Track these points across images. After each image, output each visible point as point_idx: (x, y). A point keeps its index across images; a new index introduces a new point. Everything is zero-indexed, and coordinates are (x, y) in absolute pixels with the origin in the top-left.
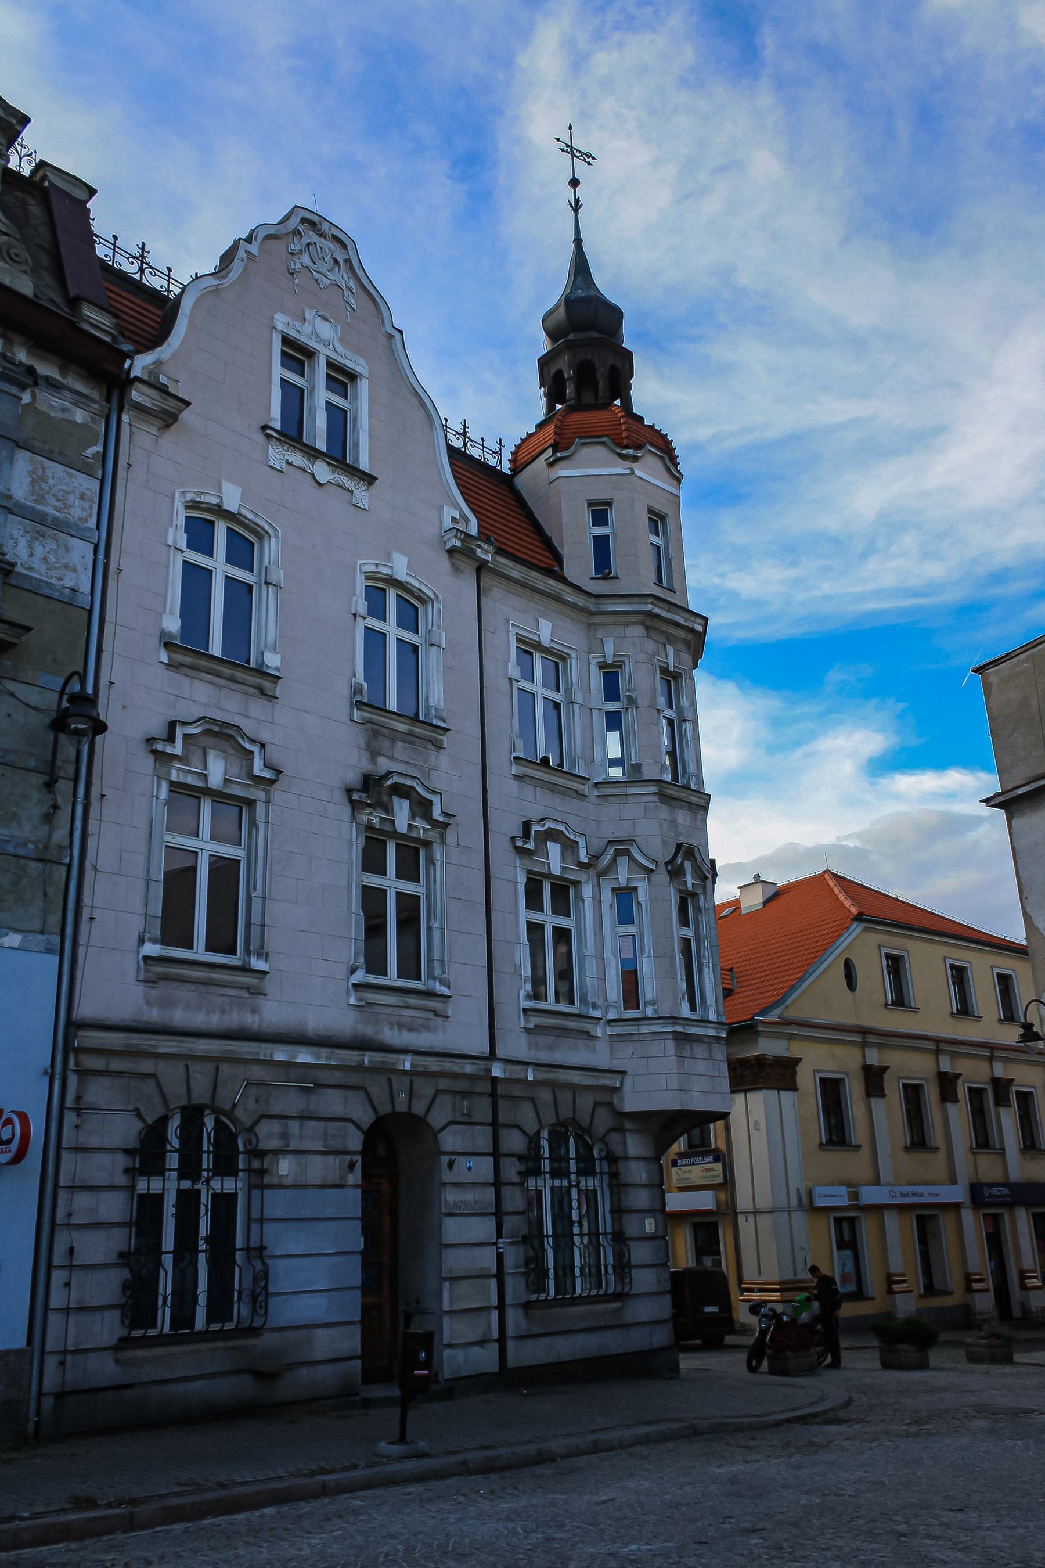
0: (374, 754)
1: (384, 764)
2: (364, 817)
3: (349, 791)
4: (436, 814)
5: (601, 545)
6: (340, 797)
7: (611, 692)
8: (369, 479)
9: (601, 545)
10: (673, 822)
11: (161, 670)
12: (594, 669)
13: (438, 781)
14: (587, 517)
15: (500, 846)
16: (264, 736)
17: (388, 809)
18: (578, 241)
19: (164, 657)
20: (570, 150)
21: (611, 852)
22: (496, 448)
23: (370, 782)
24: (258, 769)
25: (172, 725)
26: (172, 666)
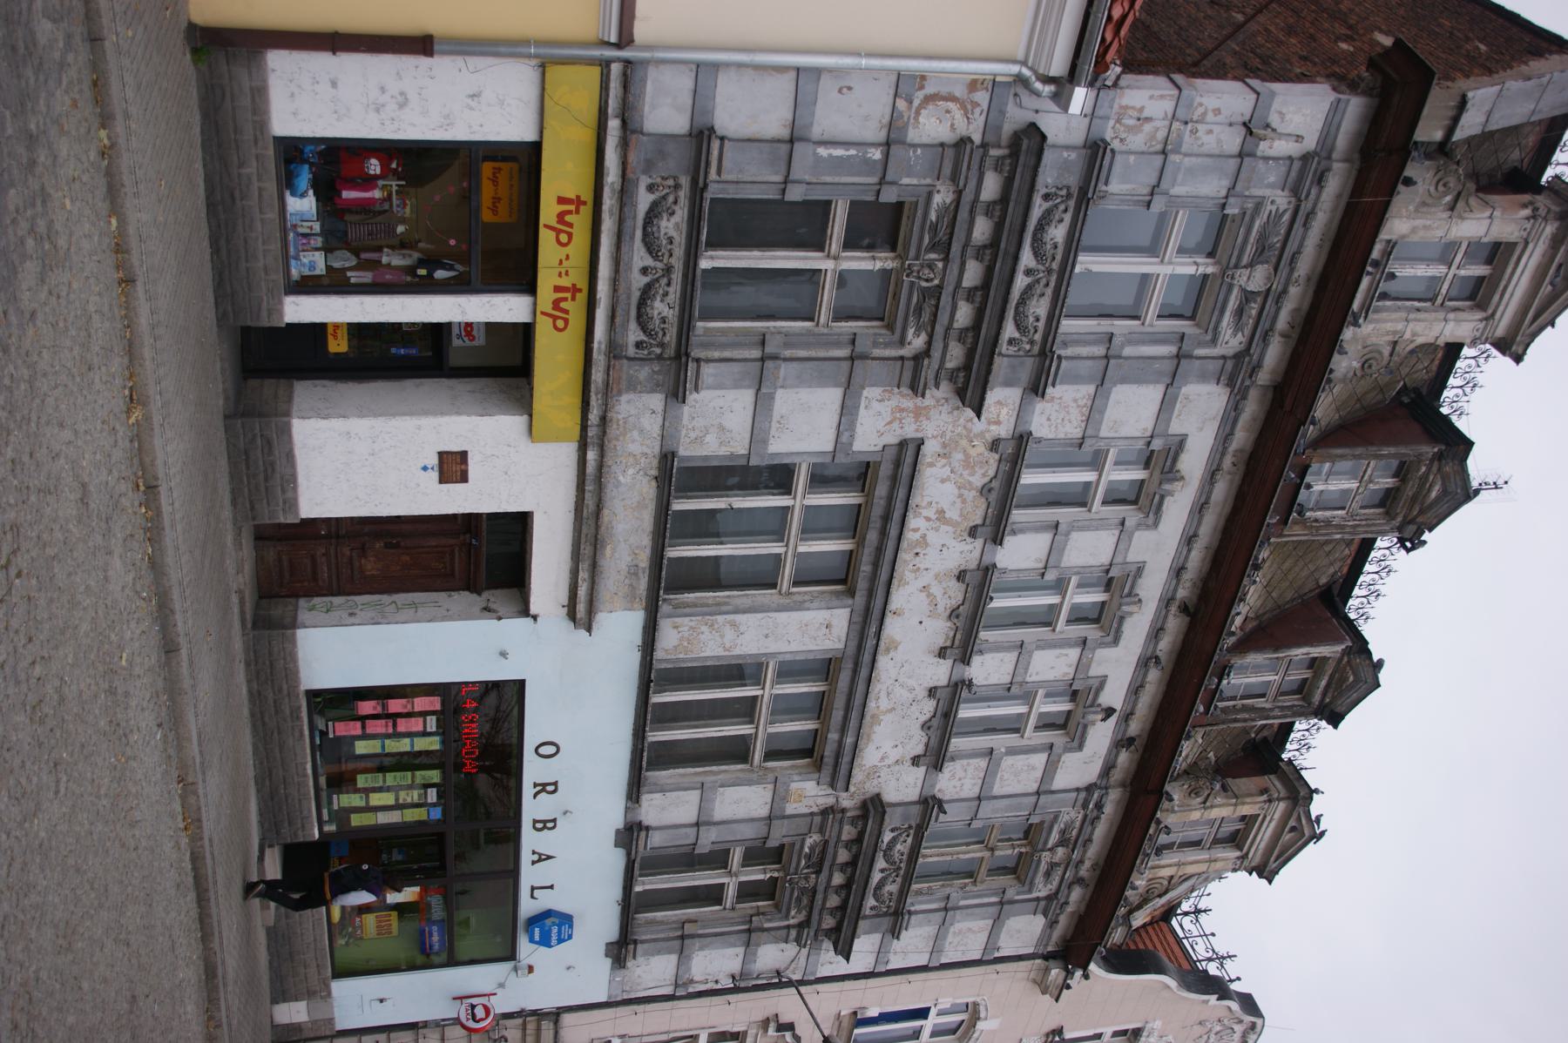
11: (834, 1011)
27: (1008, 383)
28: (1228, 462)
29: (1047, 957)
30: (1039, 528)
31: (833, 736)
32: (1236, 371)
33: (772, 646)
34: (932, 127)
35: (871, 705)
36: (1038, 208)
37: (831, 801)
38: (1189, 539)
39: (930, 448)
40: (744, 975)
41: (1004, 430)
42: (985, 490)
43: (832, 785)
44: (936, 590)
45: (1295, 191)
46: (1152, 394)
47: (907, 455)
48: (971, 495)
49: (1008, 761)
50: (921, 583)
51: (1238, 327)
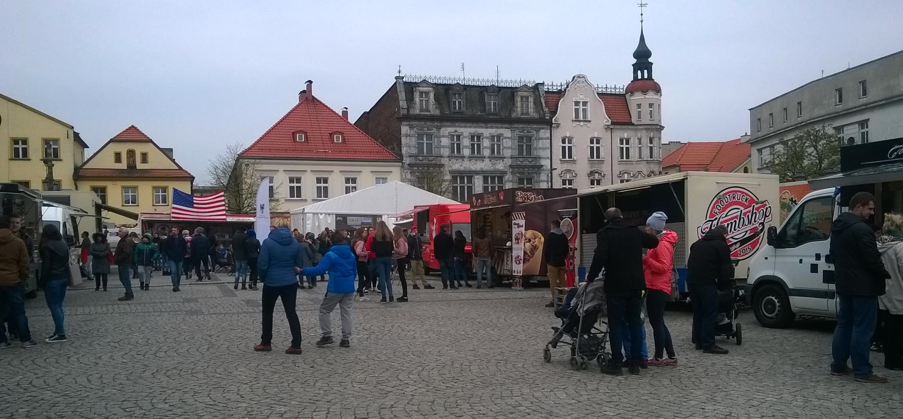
0: (592, 168)
1: (593, 169)
2: (590, 178)
3: (588, 174)
4: (602, 175)
5: (639, 112)
6: (587, 176)
7: (640, 144)
8: (590, 121)
9: (639, 112)
10: (650, 167)
12: (636, 139)
13: (603, 169)
14: (636, 107)
15: (615, 176)
16: (574, 169)
17: (594, 176)
18: (642, 31)
19: (560, 162)
20: (641, 5)
21: (638, 173)
22: (622, 87)
23: (592, 173)
24: (574, 175)
25: (562, 172)
26: (561, 163)
27: (441, 161)
28: (453, 124)
29: (551, 127)
30: (463, 151)
31: (497, 175)
32: (439, 128)
33: (481, 185)
34: (409, 176)
35: (492, 170)
36: (418, 161)
37: (510, 173)
38: (465, 127)
39: (450, 169)
40: (548, 182)
41: (448, 159)
42: (457, 160)
43: (507, 173)
44: (473, 163)
45: (413, 128)
46: (443, 139)
47: (451, 172)
48: (457, 162)
49: (505, 145)
50: (471, 166)
51: (433, 129)
